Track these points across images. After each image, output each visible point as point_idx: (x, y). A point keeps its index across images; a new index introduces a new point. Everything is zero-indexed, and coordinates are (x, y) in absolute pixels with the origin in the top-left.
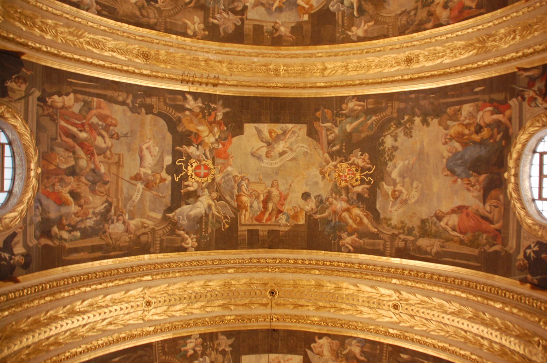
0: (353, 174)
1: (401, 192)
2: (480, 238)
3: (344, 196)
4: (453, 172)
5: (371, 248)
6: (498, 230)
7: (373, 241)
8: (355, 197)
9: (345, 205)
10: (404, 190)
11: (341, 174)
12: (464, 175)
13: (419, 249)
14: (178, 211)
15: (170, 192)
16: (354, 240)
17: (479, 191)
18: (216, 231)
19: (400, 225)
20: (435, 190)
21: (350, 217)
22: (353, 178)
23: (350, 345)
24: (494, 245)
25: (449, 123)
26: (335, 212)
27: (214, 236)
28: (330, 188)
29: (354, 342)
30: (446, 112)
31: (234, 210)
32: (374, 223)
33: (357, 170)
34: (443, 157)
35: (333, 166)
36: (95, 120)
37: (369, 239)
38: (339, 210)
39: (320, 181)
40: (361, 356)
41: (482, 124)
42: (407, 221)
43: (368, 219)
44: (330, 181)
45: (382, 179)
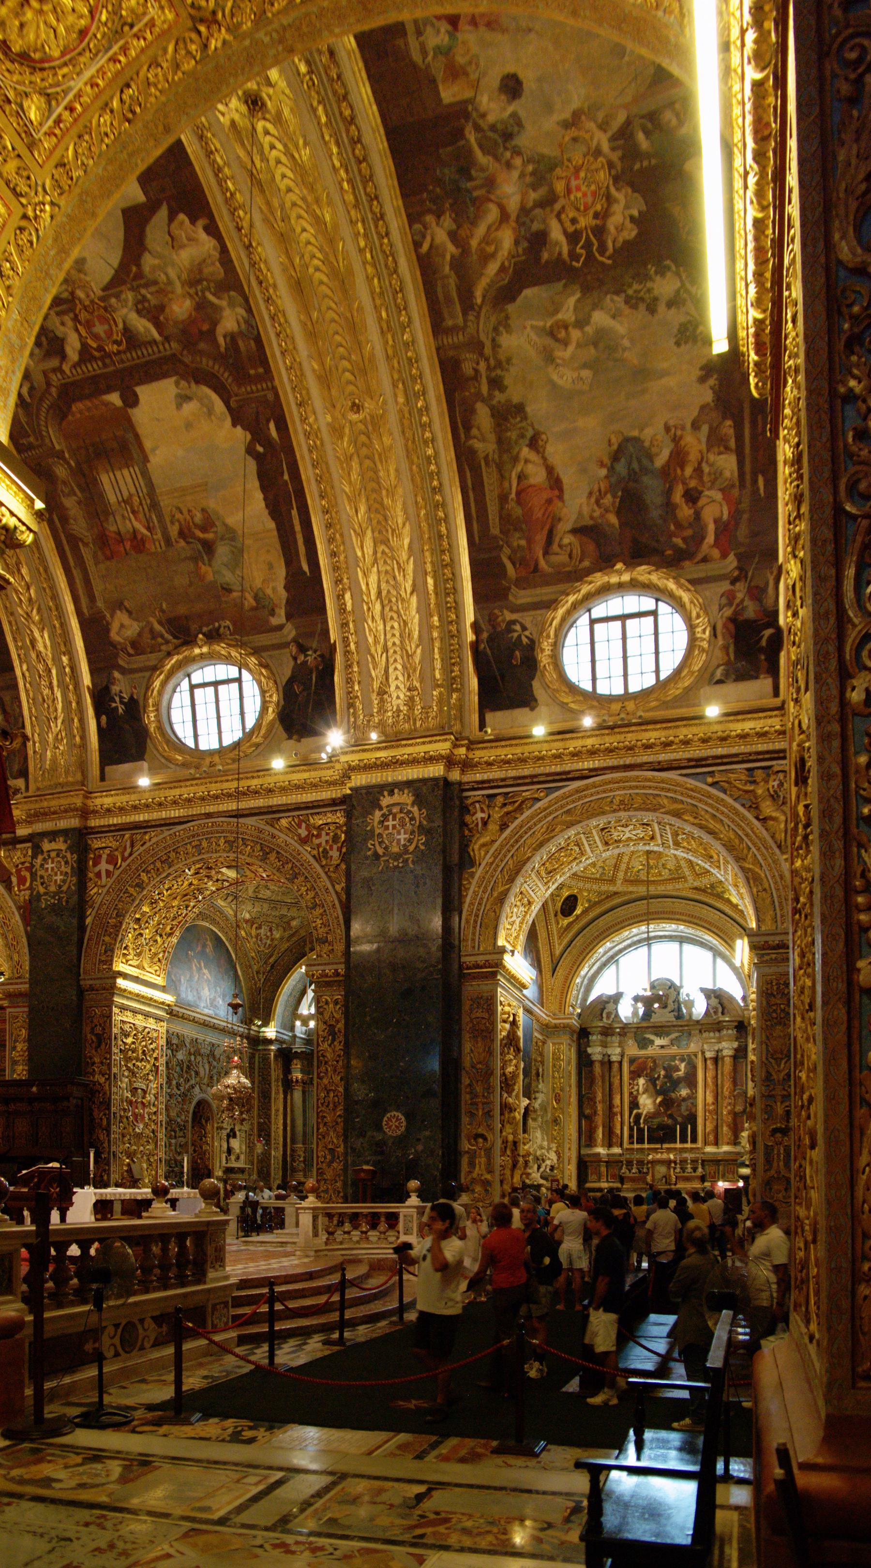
0: (587, 208)
1: (566, 343)
2: (517, 535)
4: (615, 457)
5: (441, 297)
6: (536, 569)
7: (454, 295)
11: (582, 174)
16: (445, 250)
17: (592, 518)
20: (581, 423)
21: (489, 228)
22: (578, 210)
23: (232, 305)
24: (514, 564)
28: (546, 151)
29: (241, 311)
33: (596, 216)
35: (599, 144)
37: (458, 289)
38: (498, 192)
39: (557, 117)
40: (225, 337)
42: (513, 370)
43: (497, 274)
44: (560, 146)
45: (586, 289)
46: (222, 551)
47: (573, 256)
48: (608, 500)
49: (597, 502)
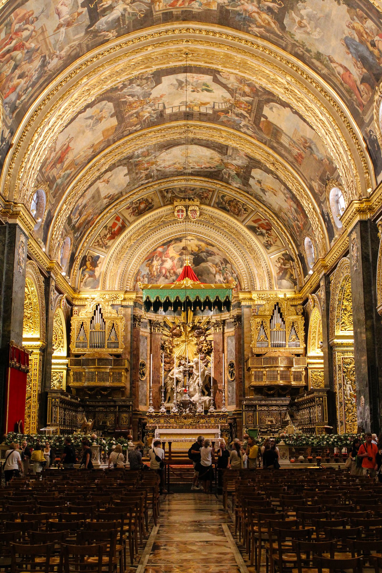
3: (255, 3)
4: (348, 47)
8: (265, 8)
9: (256, 10)
10: (308, 25)
12: (354, 56)
13: (313, 63)
14: (96, 24)
15: (88, 17)
18: (133, 21)
19: (301, 43)
25: (355, 17)
26: (246, 11)
27: (132, 24)
30: (355, 9)
31: (148, 5)
32: (280, 29)
34: (344, 33)
36: (17, 27)
41: (377, 45)
46: (313, 147)
47: (278, 4)
48: (359, 64)
49: (358, 68)
